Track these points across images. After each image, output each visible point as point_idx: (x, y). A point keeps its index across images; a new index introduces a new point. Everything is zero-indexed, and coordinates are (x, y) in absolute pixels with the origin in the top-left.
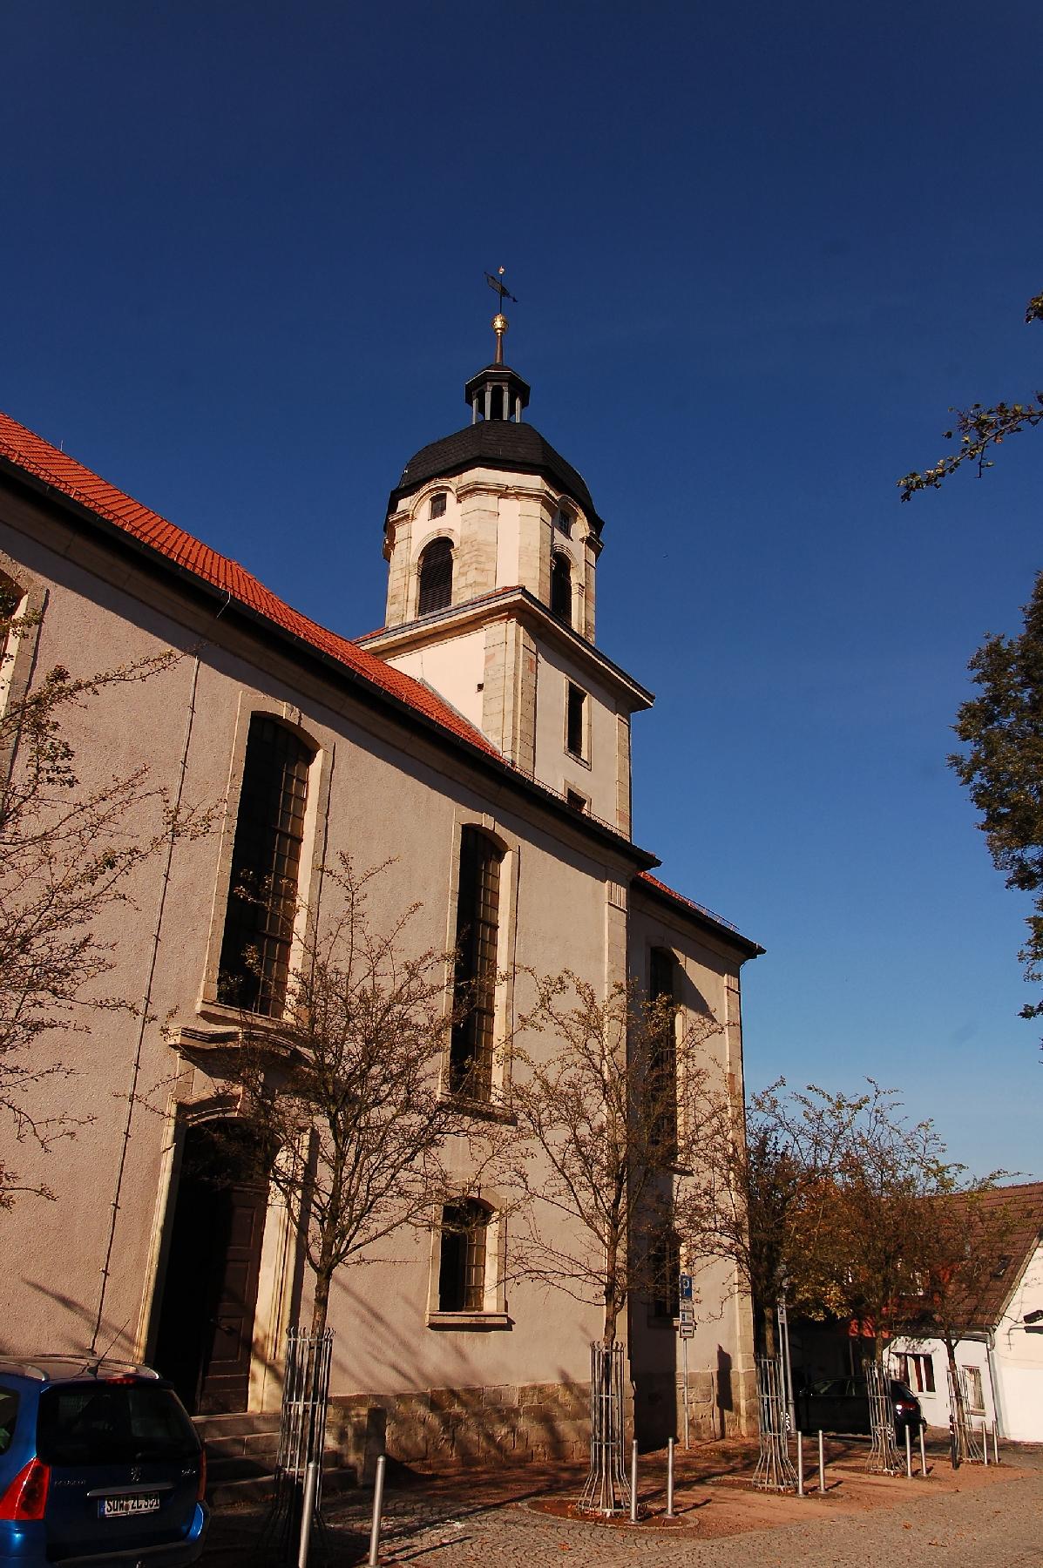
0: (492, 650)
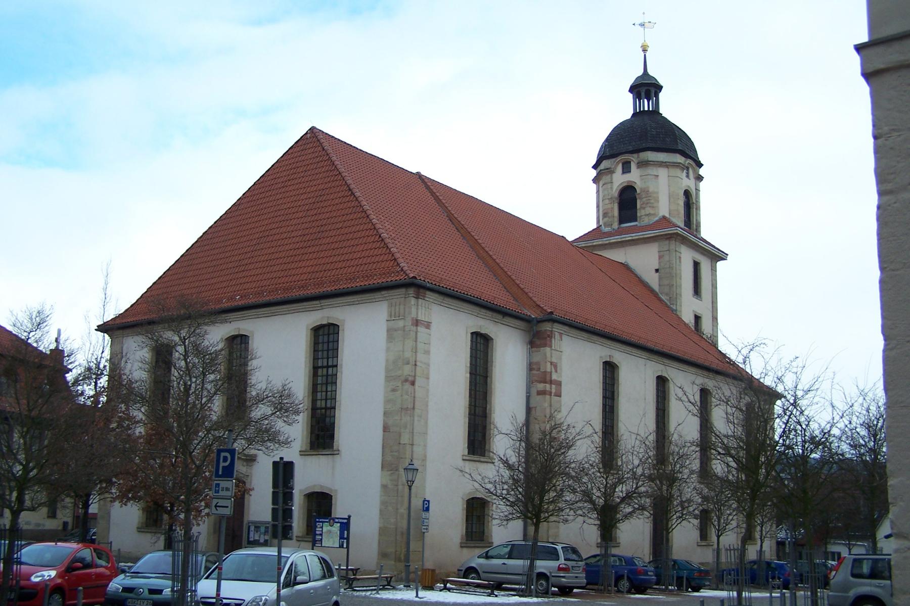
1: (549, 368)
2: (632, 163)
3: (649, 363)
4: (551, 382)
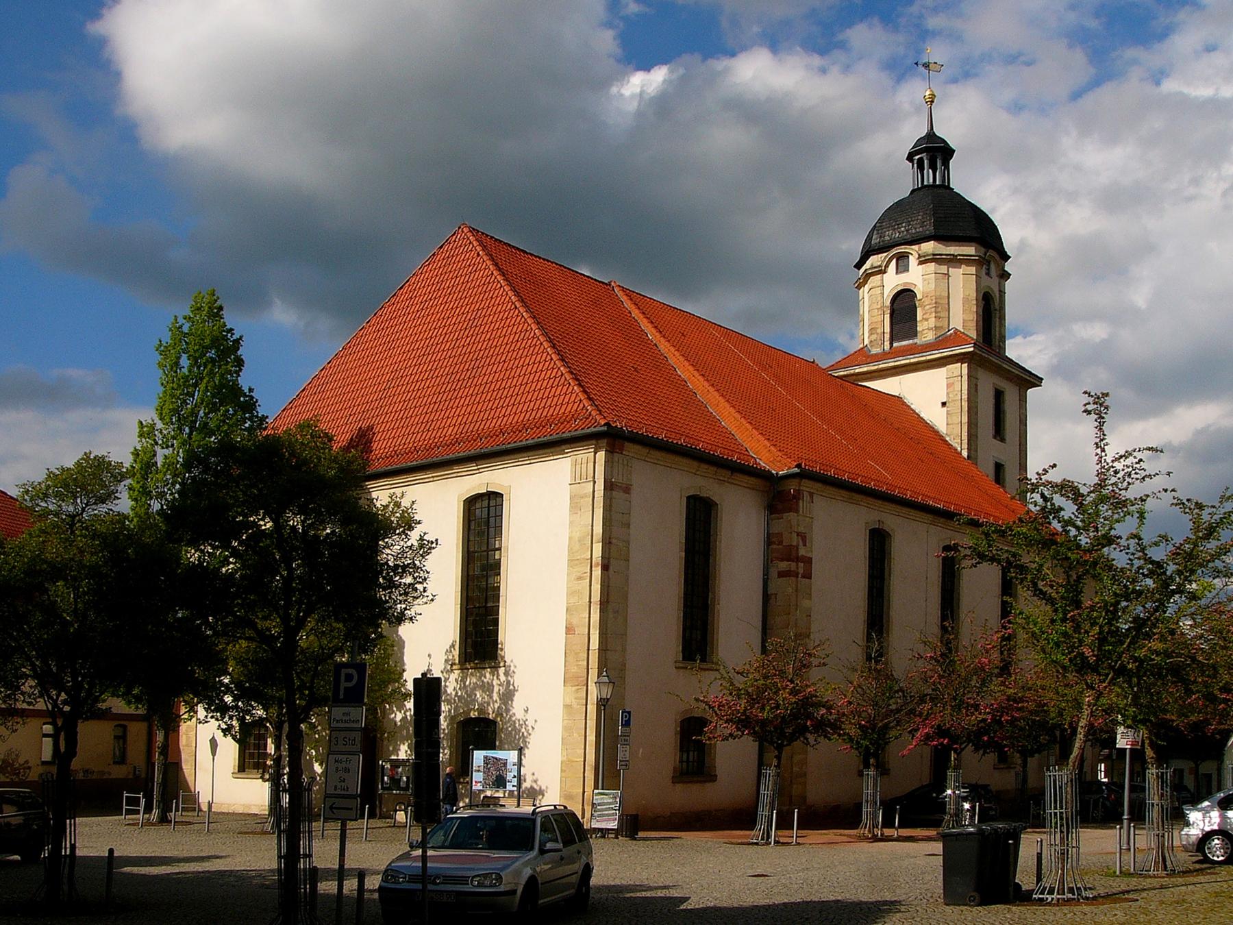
0: (951, 381)
1: (795, 540)
2: (910, 256)
3: (932, 529)
4: (798, 559)
